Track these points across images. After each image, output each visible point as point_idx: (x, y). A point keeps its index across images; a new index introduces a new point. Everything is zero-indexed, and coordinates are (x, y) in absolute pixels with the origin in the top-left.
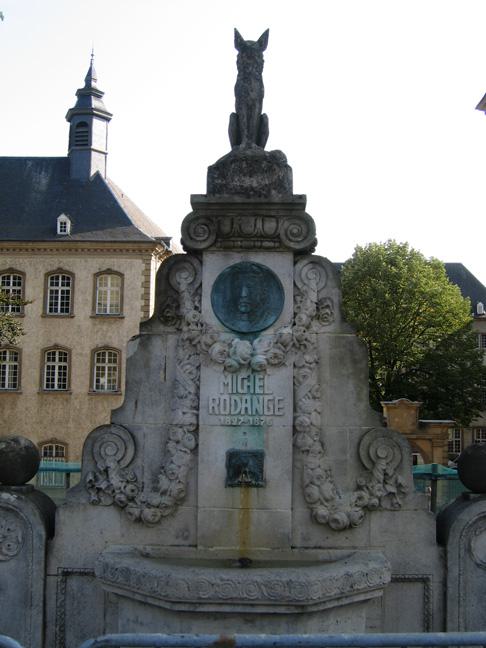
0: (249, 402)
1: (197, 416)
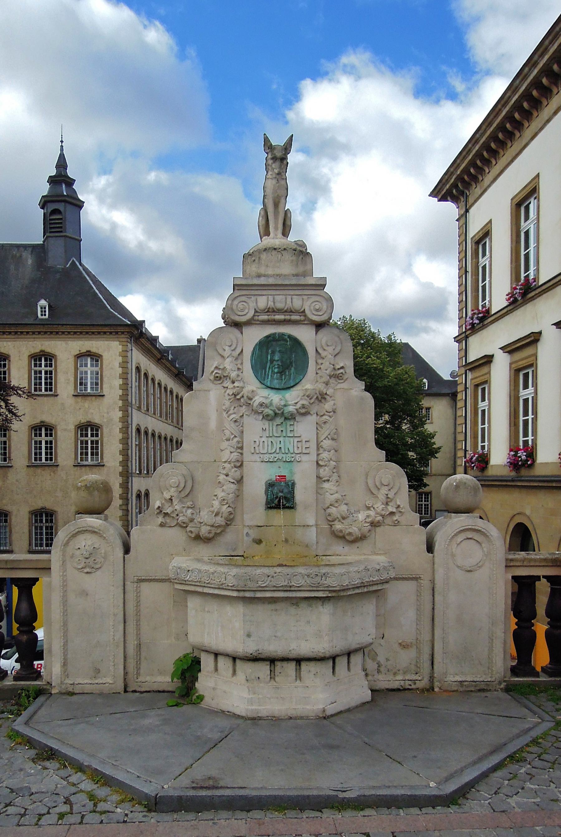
1: (242, 454)
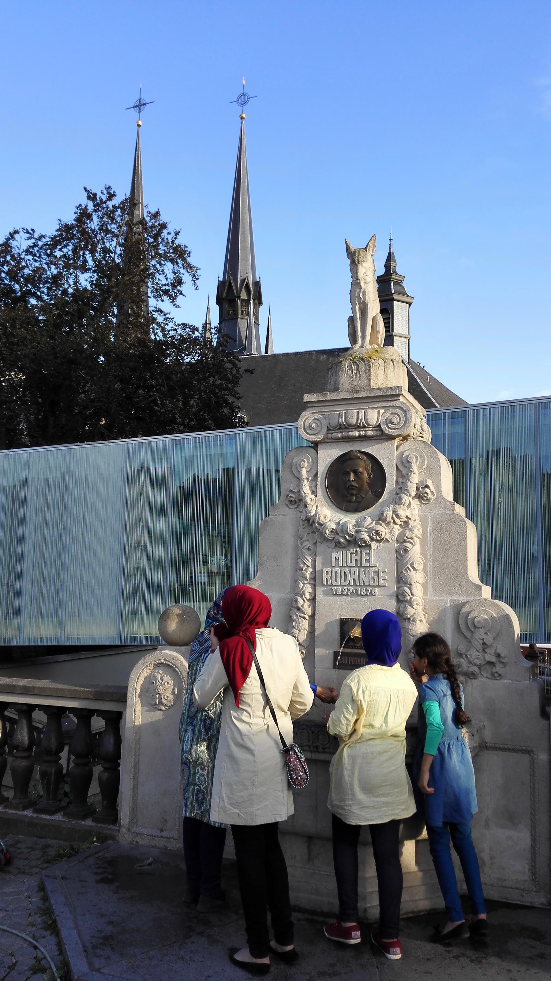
0: (357, 573)
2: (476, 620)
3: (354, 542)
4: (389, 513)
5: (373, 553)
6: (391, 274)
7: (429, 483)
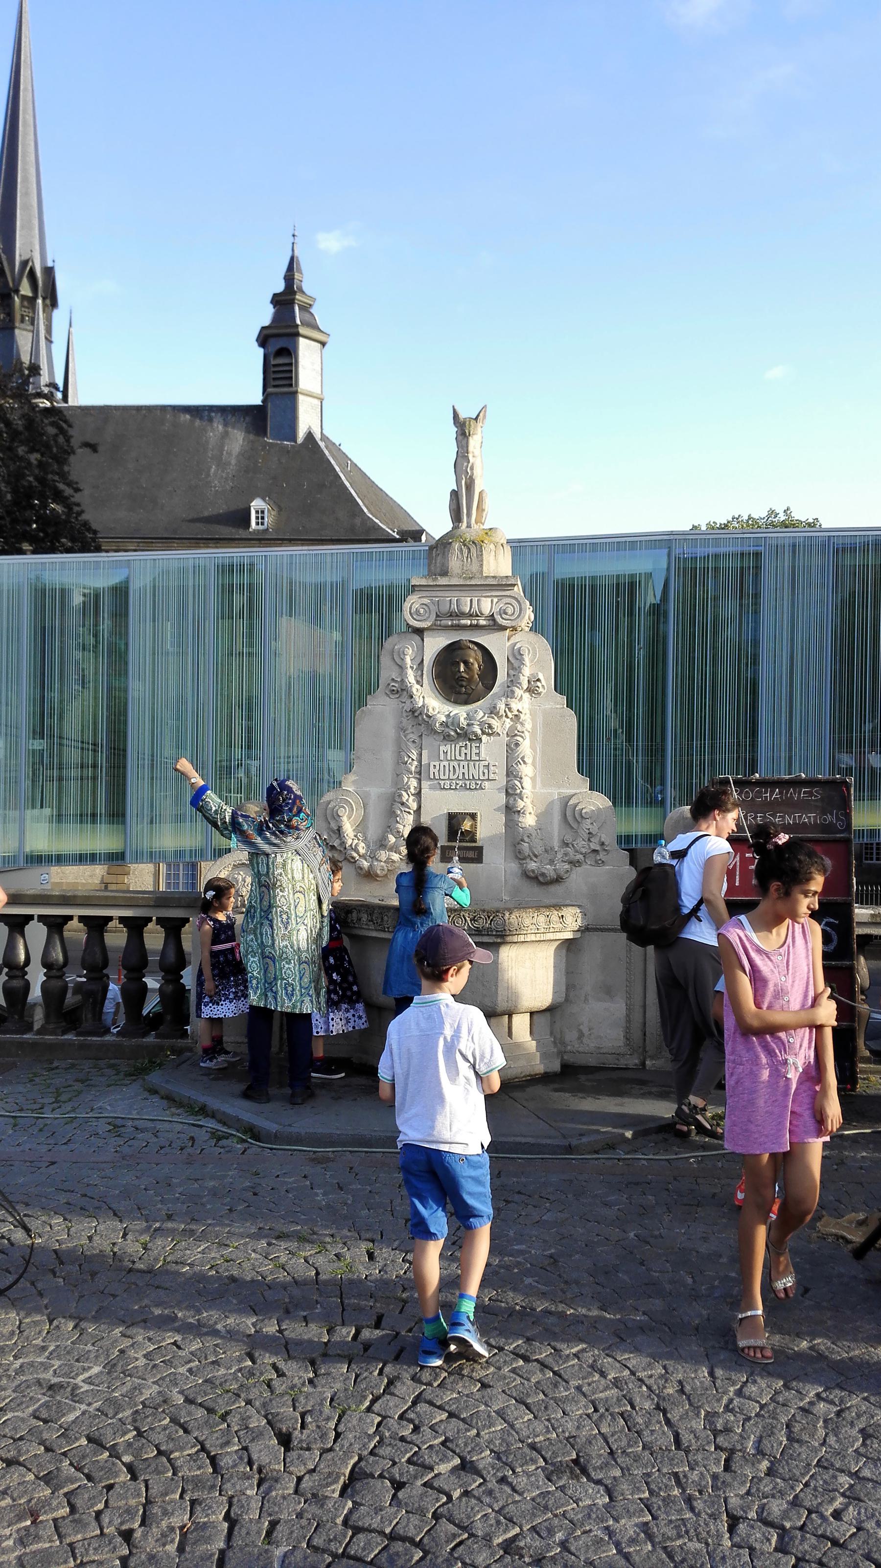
0: (466, 767)
2: (584, 811)
3: (465, 735)
4: (501, 706)
5: (483, 746)
6: (295, 293)
7: (541, 676)
